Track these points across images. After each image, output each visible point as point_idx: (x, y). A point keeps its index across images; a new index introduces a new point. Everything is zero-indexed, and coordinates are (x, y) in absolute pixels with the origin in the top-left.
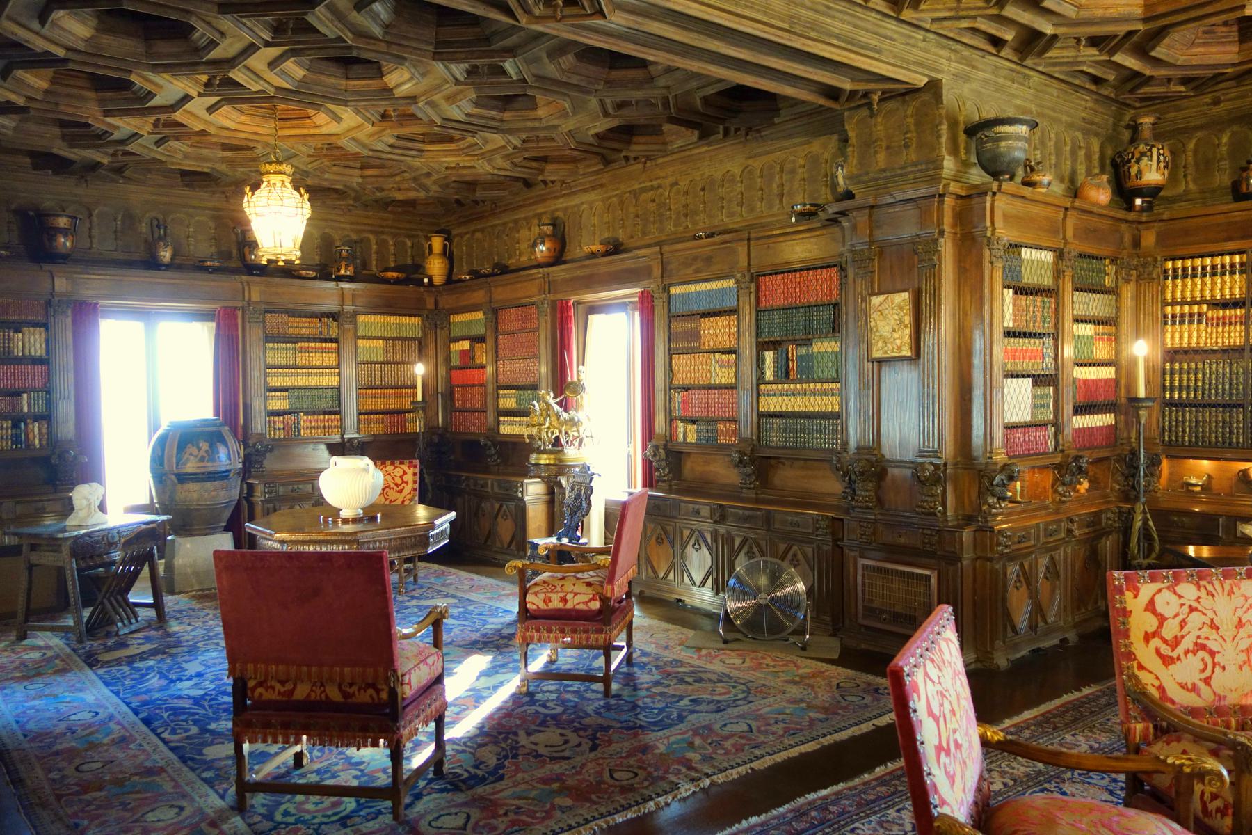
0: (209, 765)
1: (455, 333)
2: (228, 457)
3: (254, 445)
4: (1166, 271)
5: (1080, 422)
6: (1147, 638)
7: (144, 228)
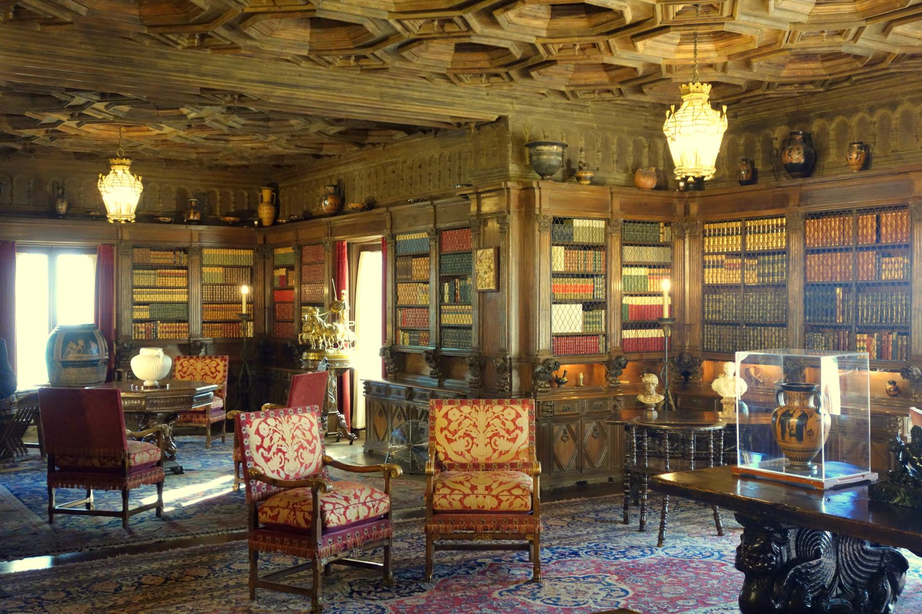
0: (42, 510)
1: (277, 263)
2: (98, 351)
3: (123, 344)
4: (704, 231)
5: (629, 334)
6: (442, 430)
7: (48, 188)
